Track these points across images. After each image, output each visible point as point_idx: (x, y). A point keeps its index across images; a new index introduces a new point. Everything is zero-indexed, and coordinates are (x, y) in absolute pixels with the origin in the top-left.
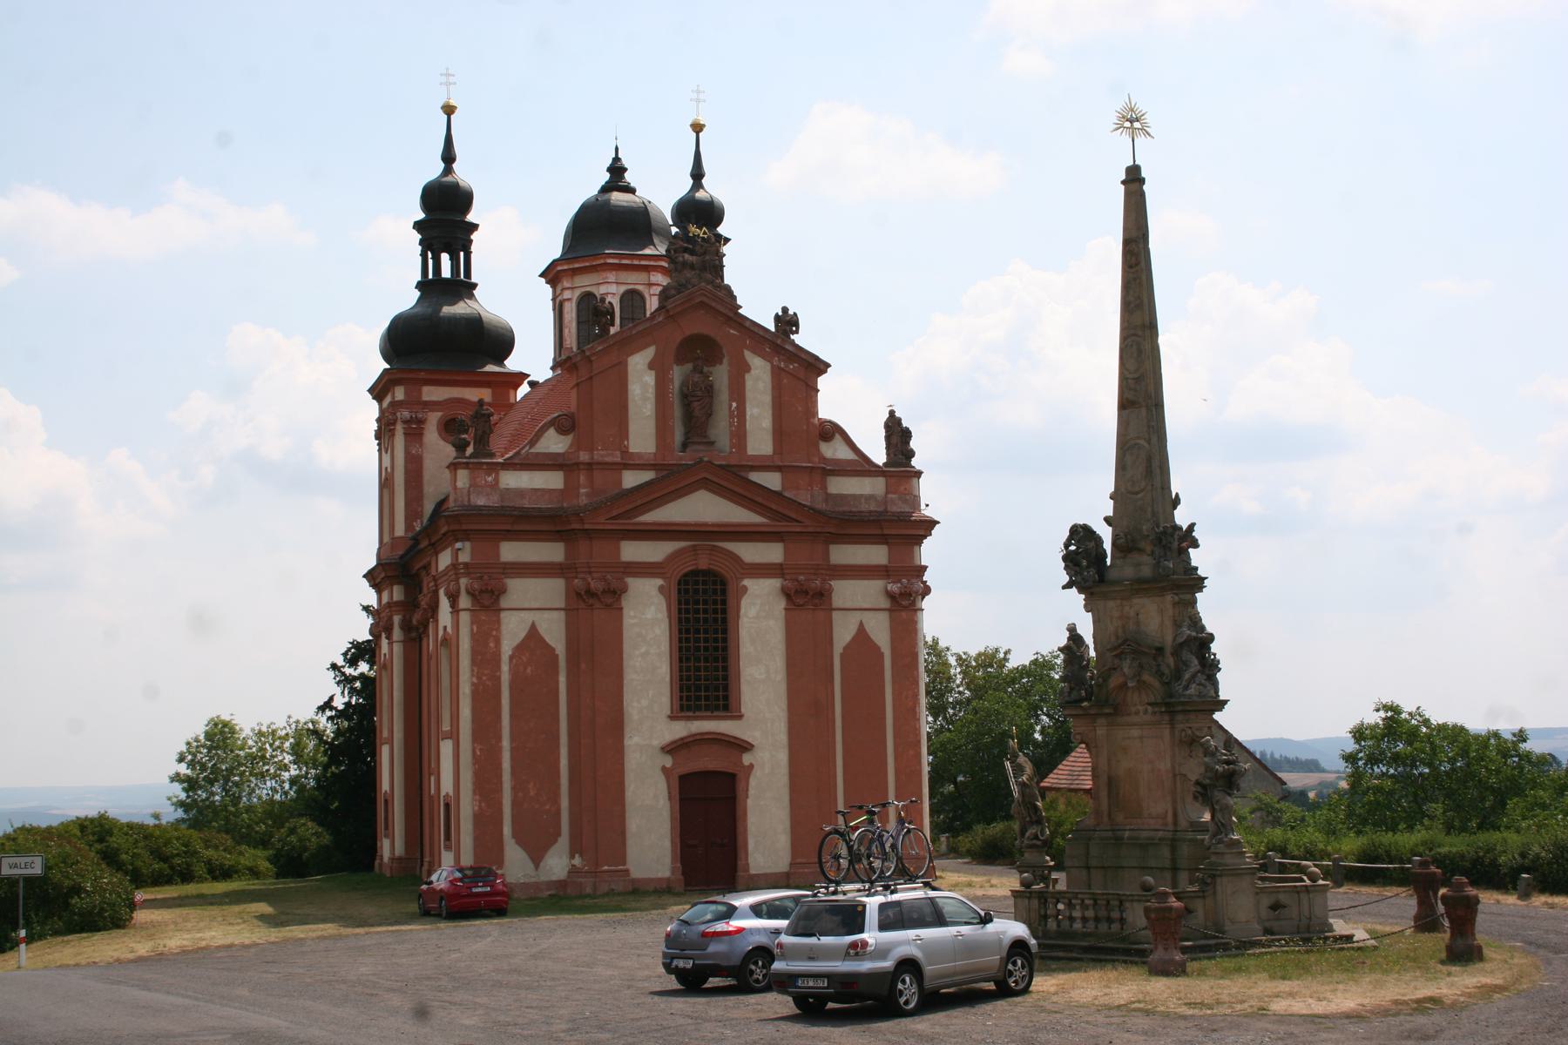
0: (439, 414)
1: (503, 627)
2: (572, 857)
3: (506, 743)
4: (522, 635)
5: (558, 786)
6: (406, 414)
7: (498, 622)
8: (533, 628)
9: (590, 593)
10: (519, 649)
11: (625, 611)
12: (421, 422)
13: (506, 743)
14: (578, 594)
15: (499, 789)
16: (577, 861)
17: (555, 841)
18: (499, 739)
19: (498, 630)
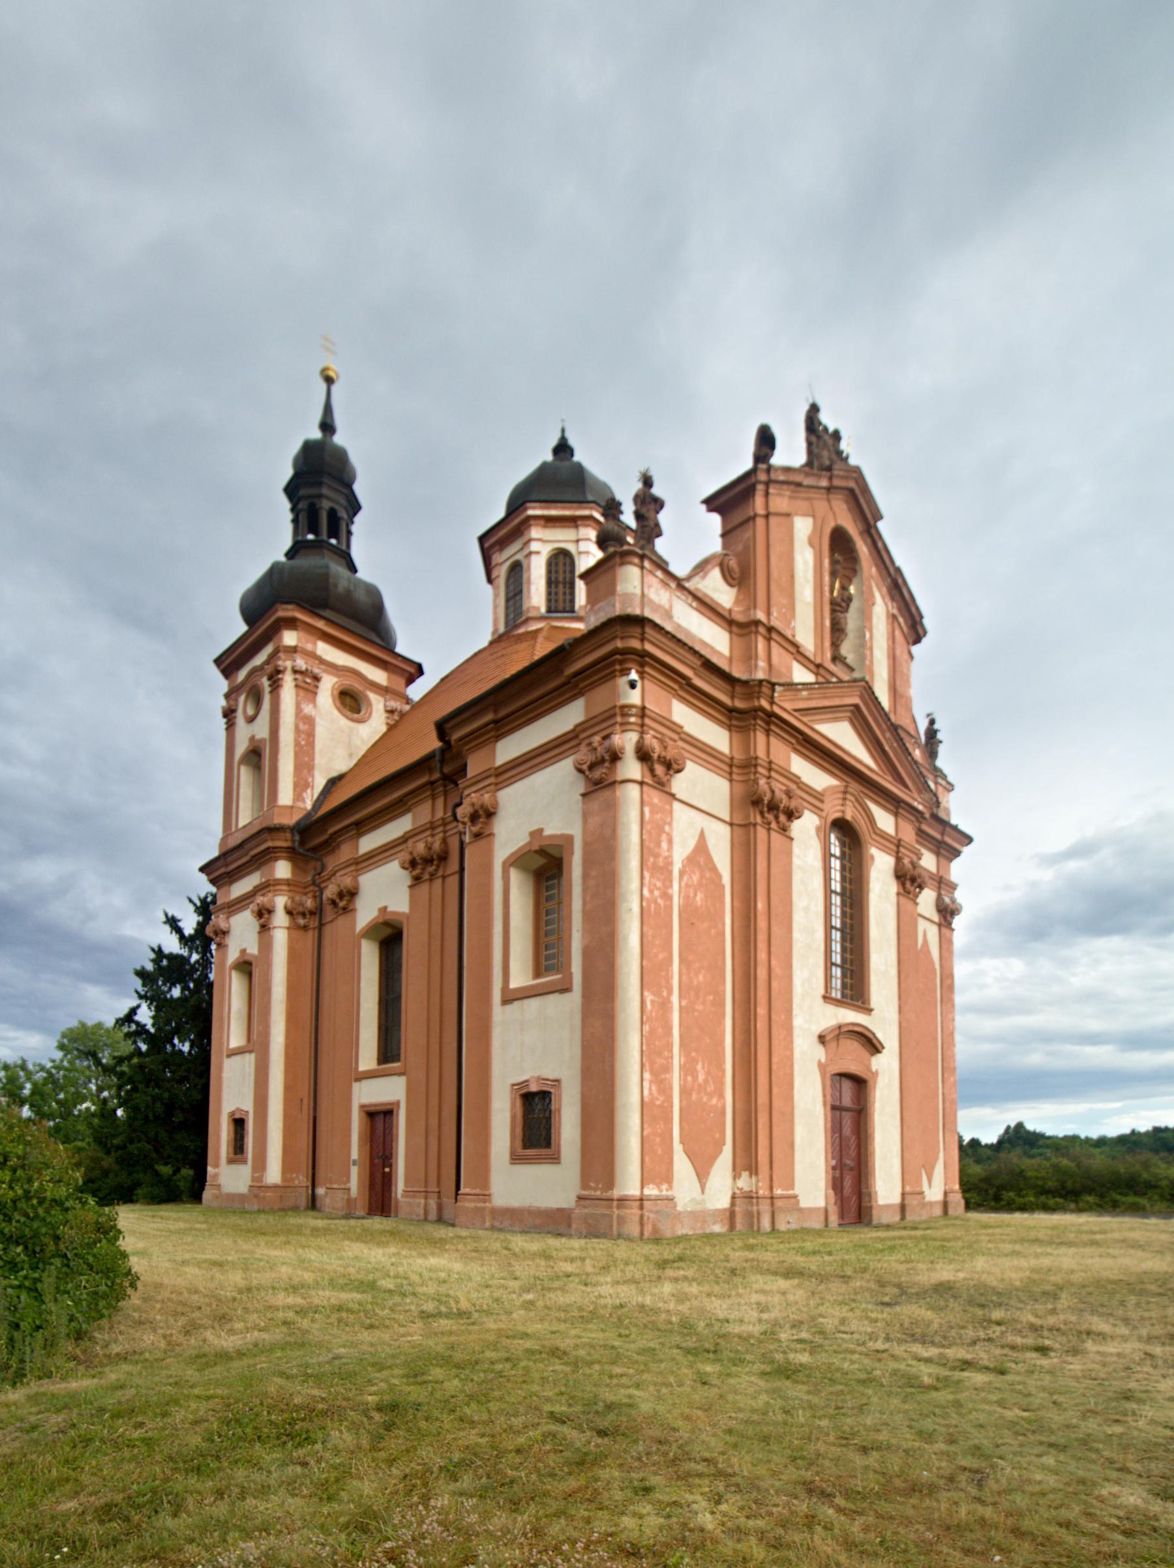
0: (335, 680)
1: (675, 824)
2: (736, 1176)
3: (675, 999)
4: (692, 844)
5: (723, 1071)
6: (301, 663)
7: (671, 812)
8: (702, 835)
9: (773, 807)
10: (691, 860)
11: (795, 843)
12: (317, 679)
13: (675, 999)
14: (756, 802)
15: (667, 1069)
16: (745, 1182)
17: (721, 1151)
18: (670, 992)
19: (670, 824)
